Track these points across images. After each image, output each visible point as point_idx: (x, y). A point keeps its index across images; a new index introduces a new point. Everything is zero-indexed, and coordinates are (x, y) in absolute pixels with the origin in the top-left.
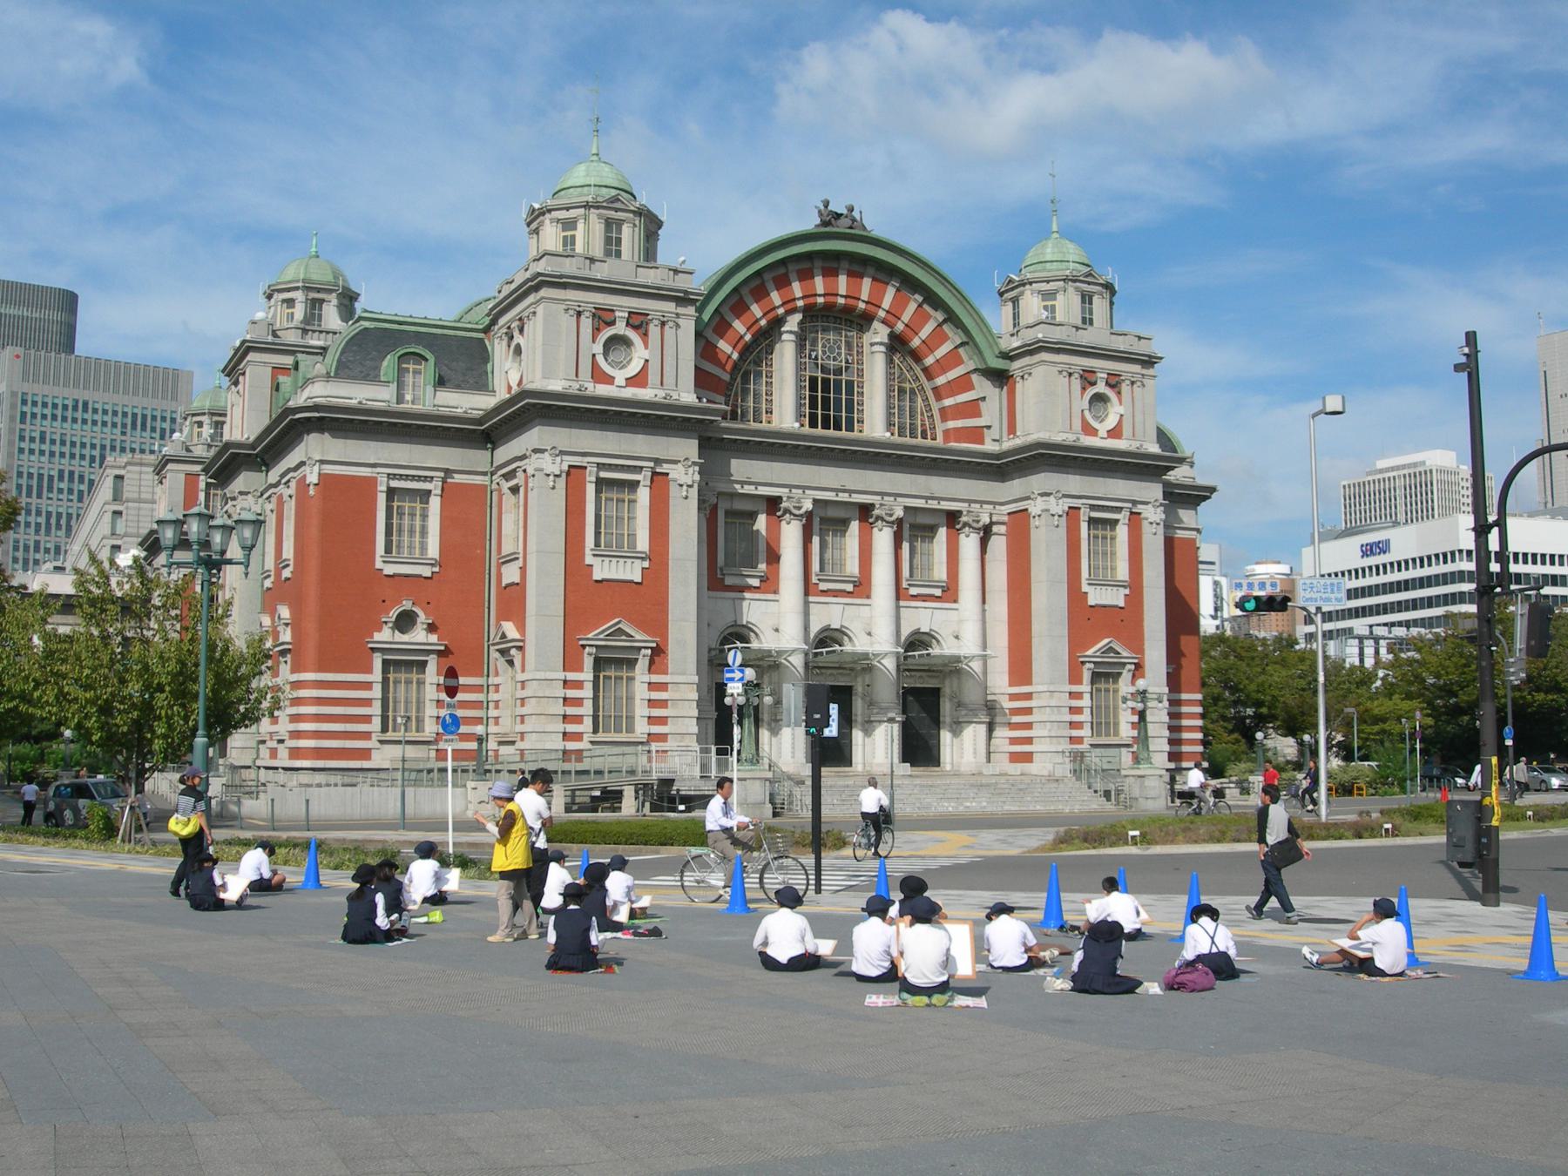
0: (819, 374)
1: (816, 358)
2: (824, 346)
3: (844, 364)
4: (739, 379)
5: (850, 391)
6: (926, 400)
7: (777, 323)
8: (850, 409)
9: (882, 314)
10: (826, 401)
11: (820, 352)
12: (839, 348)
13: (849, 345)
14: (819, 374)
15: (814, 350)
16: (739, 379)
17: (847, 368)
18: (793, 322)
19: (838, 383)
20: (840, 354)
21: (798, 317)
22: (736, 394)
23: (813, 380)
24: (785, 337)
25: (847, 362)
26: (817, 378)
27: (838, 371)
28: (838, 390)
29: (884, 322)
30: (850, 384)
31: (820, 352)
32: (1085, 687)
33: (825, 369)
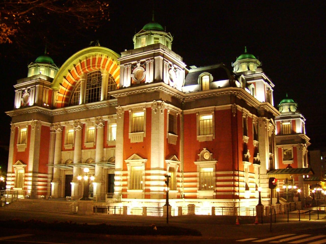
1: (91, 84)
4: (73, 96)
10: (92, 95)
11: (92, 82)
12: (96, 80)
15: (90, 82)
16: (73, 96)
19: (95, 89)
22: (73, 99)
25: (98, 83)
27: (96, 86)
28: (95, 91)
30: (98, 89)
31: (92, 82)
33: (93, 87)
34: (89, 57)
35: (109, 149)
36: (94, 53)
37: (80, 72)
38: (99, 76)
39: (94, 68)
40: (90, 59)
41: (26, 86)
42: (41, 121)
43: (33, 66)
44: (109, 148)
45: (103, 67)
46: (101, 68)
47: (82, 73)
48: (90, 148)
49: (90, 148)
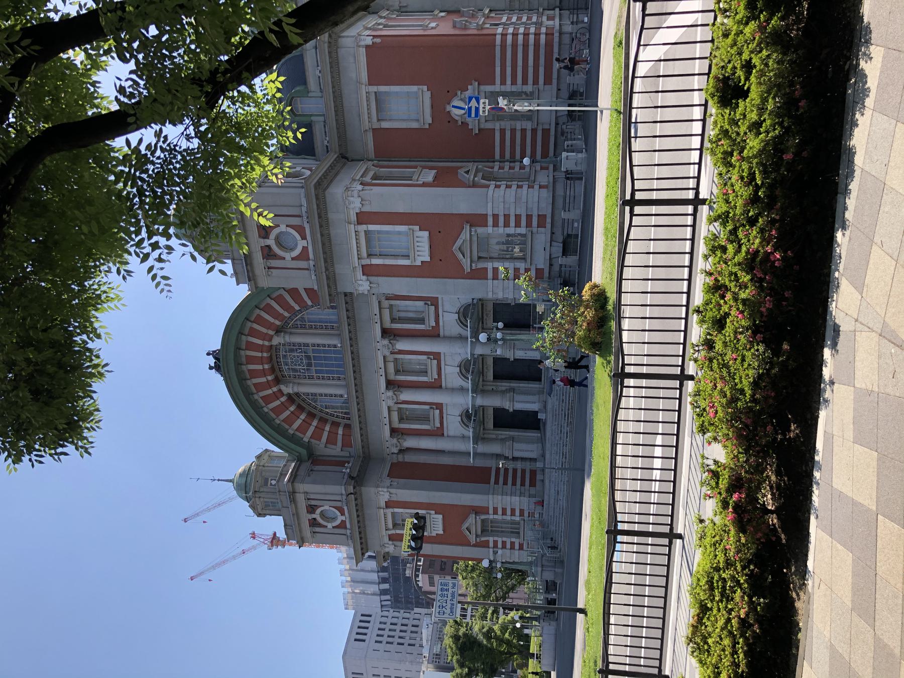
1: (304, 369)
2: (296, 365)
7: (291, 398)
9: (266, 343)
13: (292, 351)
14: (313, 368)
17: (305, 353)
18: (287, 389)
21: (283, 388)
22: (335, 412)
24: (296, 390)
27: (308, 358)
28: (320, 358)
29: (270, 340)
32: (490, 266)
33: (309, 365)
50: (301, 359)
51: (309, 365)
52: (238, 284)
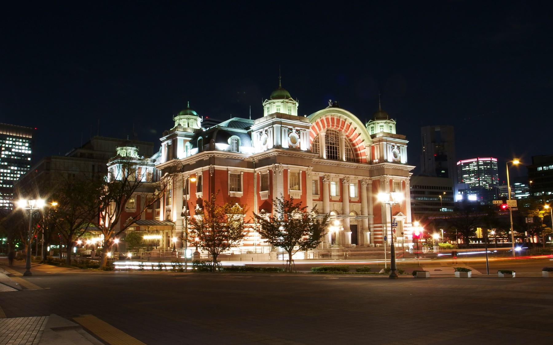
0: (330, 145)
1: (329, 141)
2: (330, 138)
3: (335, 142)
5: (336, 149)
6: (352, 151)
8: (336, 154)
10: (331, 151)
12: (334, 138)
13: (336, 138)
14: (330, 145)
15: (327, 139)
19: (333, 147)
20: (334, 140)
23: (328, 146)
26: (329, 146)
27: (334, 144)
28: (334, 149)
30: (336, 147)
31: (329, 138)
33: (331, 144)
34: (334, 115)
35: (352, 204)
36: (339, 115)
37: (325, 127)
38: (337, 135)
39: (337, 128)
40: (334, 118)
41: (294, 126)
42: (282, 164)
43: (292, 103)
44: (351, 203)
45: (346, 131)
46: (343, 131)
47: (326, 127)
48: (335, 201)
49: (335, 201)
50: (333, 141)
51: (331, 144)
52: (351, 123)
